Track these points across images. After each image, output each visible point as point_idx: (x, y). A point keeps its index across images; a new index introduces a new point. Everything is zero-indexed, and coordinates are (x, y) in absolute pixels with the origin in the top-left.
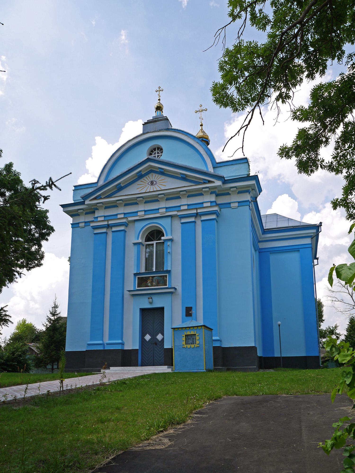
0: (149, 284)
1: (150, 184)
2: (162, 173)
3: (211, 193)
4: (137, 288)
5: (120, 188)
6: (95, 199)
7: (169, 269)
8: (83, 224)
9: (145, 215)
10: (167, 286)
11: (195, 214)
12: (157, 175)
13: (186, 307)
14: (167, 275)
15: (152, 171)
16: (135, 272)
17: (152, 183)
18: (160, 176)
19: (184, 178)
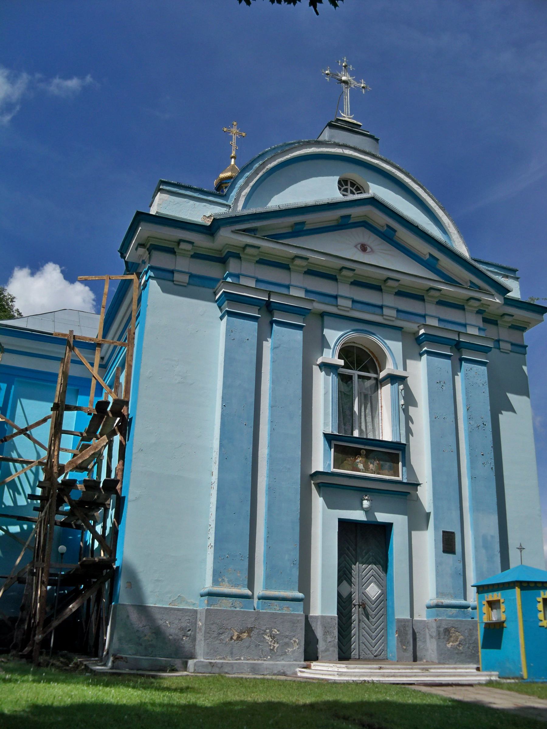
0: (361, 466)
1: (359, 246)
2: (388, 237)
3: (479, 312)
4: (333, 470)
5: (298, 231)
6: (246, 231)
7: (403, 441)
8: (186, 278)
9: (352, 309)
10: (399, 478)
11: (455, 342)
12: (374, 237)
13: (444, 532)
14: (400, 453)
15: (365, 224)
16: (329, 431)
17: (364, 248)
18: (379, 240)
19: (430, 264)
